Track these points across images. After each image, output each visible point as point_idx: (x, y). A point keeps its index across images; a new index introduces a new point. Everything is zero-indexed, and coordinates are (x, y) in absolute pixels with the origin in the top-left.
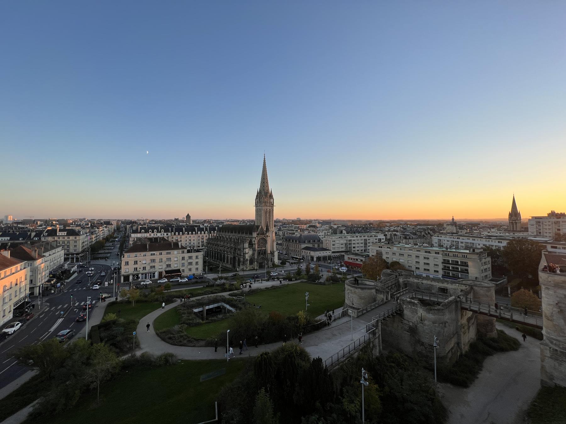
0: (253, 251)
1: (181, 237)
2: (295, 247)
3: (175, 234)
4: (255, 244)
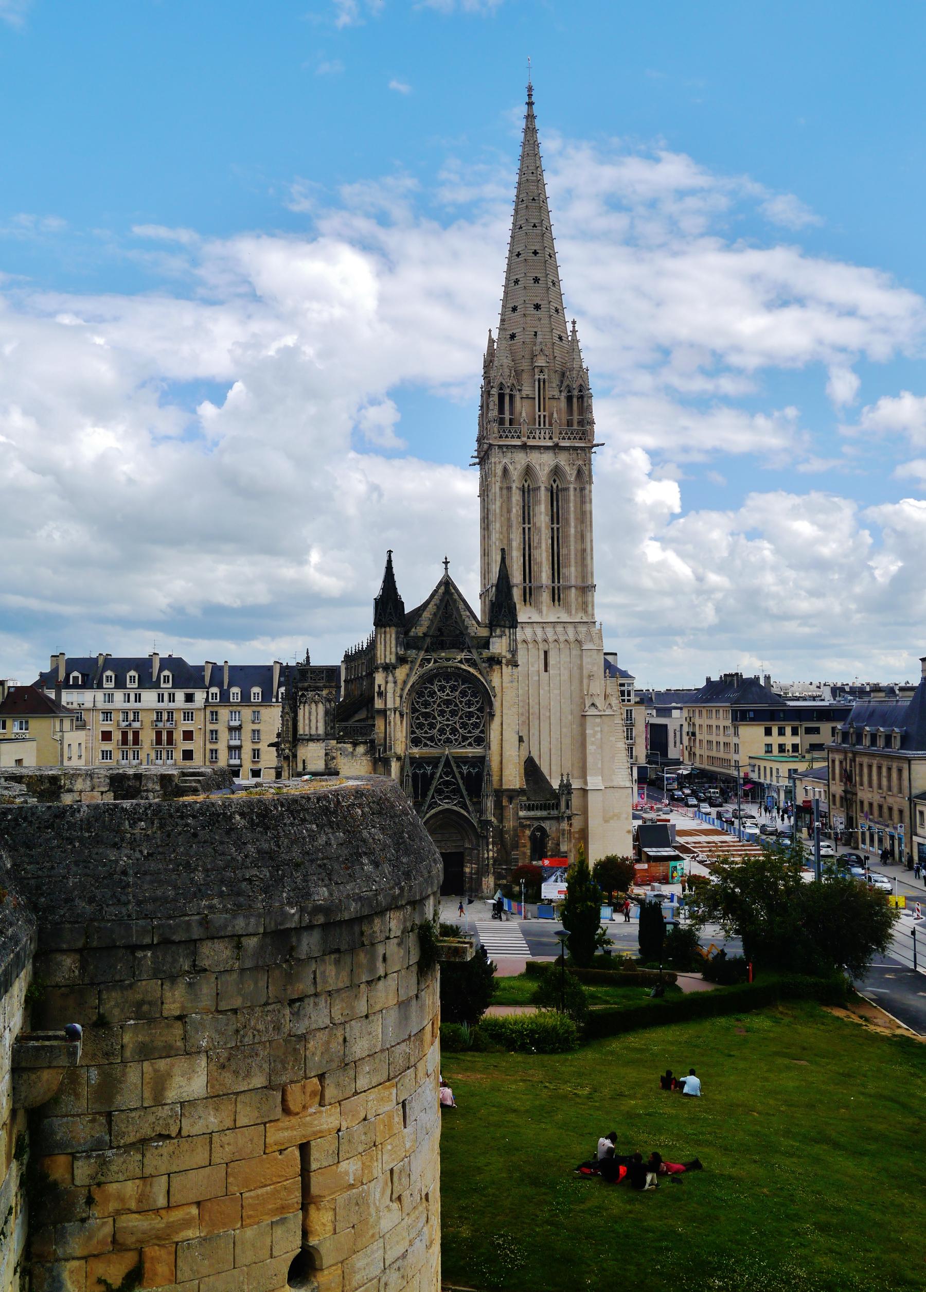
1: (256, 714)
2: (884, 782)
3: (225, 697)
4: (383, 712)
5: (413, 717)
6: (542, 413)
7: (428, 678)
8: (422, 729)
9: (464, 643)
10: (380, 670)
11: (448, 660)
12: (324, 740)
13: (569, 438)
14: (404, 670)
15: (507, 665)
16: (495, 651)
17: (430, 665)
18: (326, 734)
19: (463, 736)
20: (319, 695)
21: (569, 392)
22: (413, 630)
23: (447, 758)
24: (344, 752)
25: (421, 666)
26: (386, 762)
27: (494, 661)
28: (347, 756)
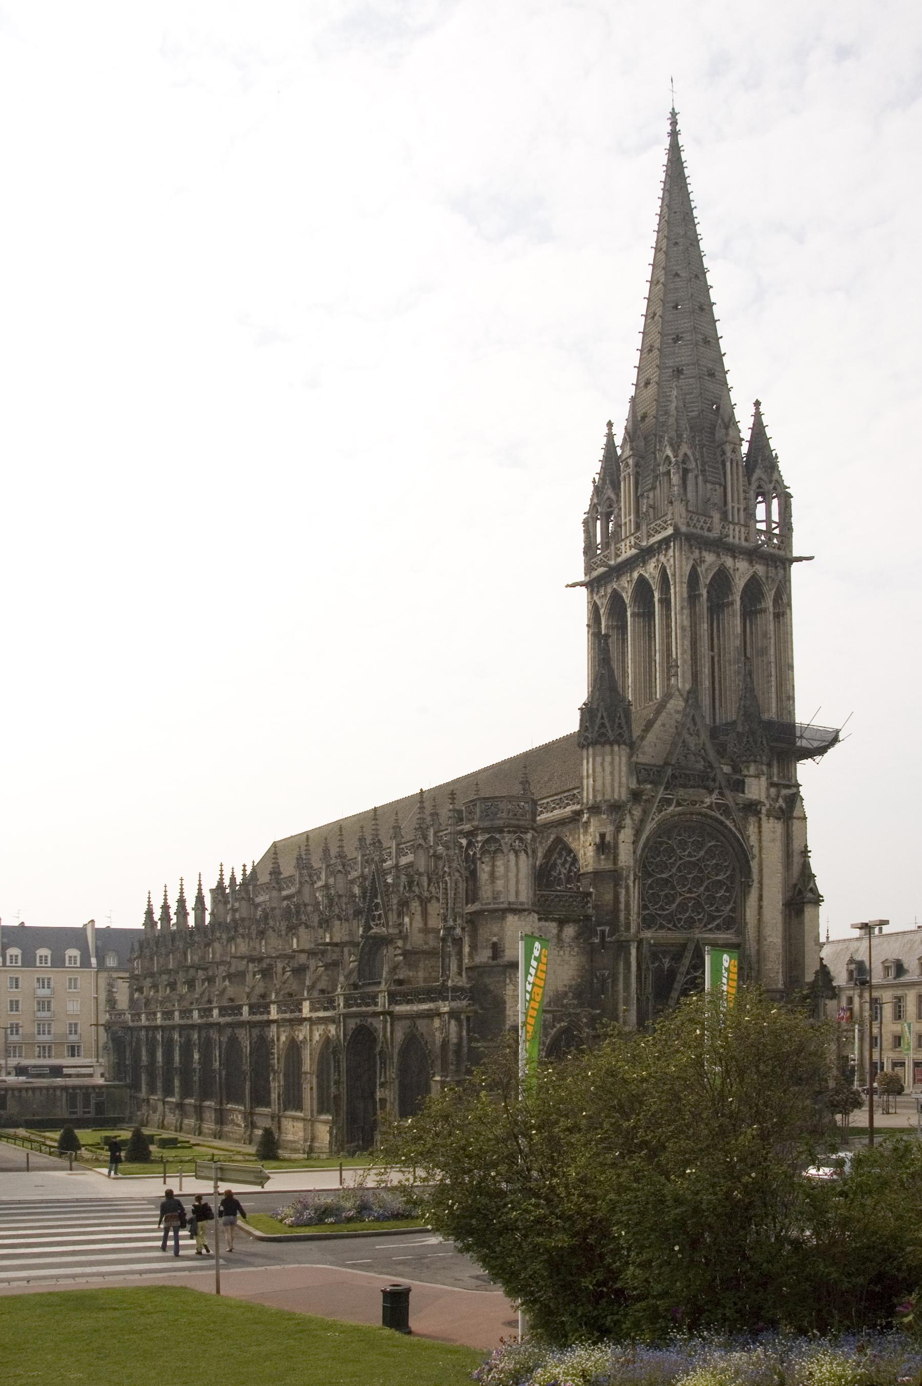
9: (714, 780)
11: (694, 803)
17: (672, 808)
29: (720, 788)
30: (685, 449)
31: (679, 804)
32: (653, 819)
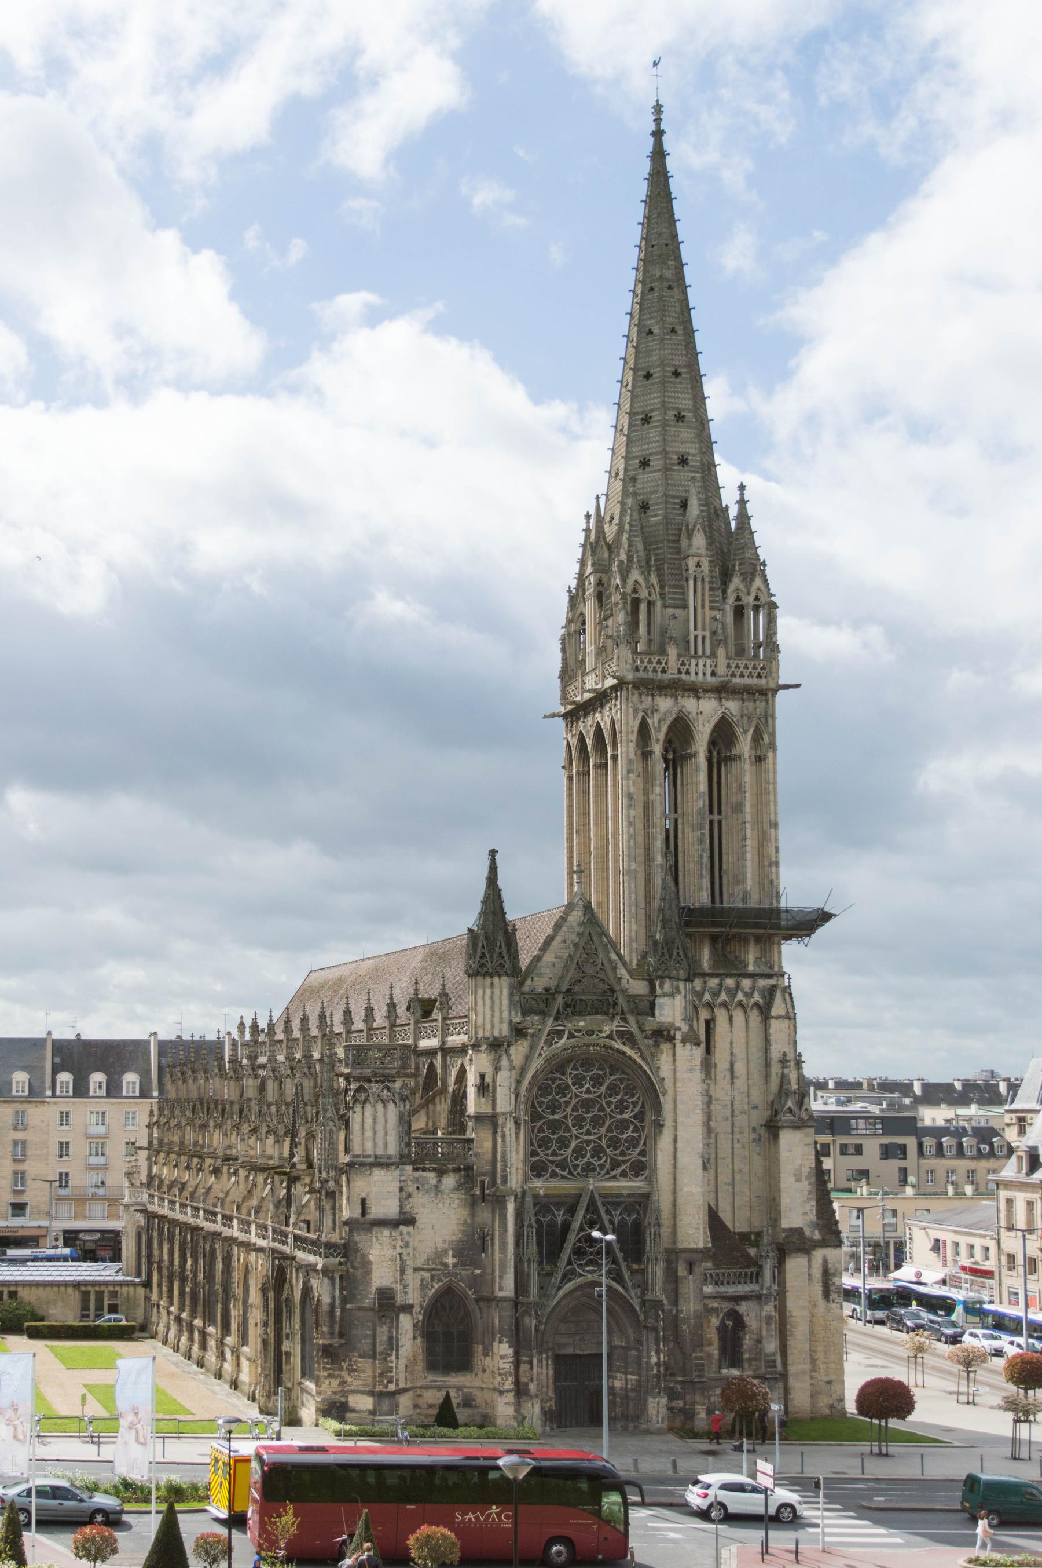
0: (473, 1203)
5: (533, 1128)
6: (700, 633)
7: (558, 1065)
8: (548, 1148)
9: (615, 1004)
10: (484, 1047)
11: (589, 1033)
12: (397, 1165)
13: (742, 676)
14: (521, 1049)
15: (684, 1041)
16: (663, 1019)
18: (402, 1156)
19: (612, 1159)
20: (389, 1089)
21: (738, 599)
22: (528, 982)
23: (592, 1197)
24: (423, 1185)
25: (549, 1043)
26: (499, 1202)
27: (663, 1035)
28: (428, 1191)
29: (623, 1013)
30: (635, 575)
31: (571, 1036)
32: (540, 1055)
